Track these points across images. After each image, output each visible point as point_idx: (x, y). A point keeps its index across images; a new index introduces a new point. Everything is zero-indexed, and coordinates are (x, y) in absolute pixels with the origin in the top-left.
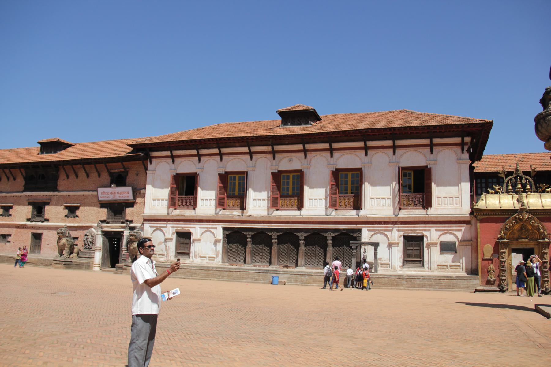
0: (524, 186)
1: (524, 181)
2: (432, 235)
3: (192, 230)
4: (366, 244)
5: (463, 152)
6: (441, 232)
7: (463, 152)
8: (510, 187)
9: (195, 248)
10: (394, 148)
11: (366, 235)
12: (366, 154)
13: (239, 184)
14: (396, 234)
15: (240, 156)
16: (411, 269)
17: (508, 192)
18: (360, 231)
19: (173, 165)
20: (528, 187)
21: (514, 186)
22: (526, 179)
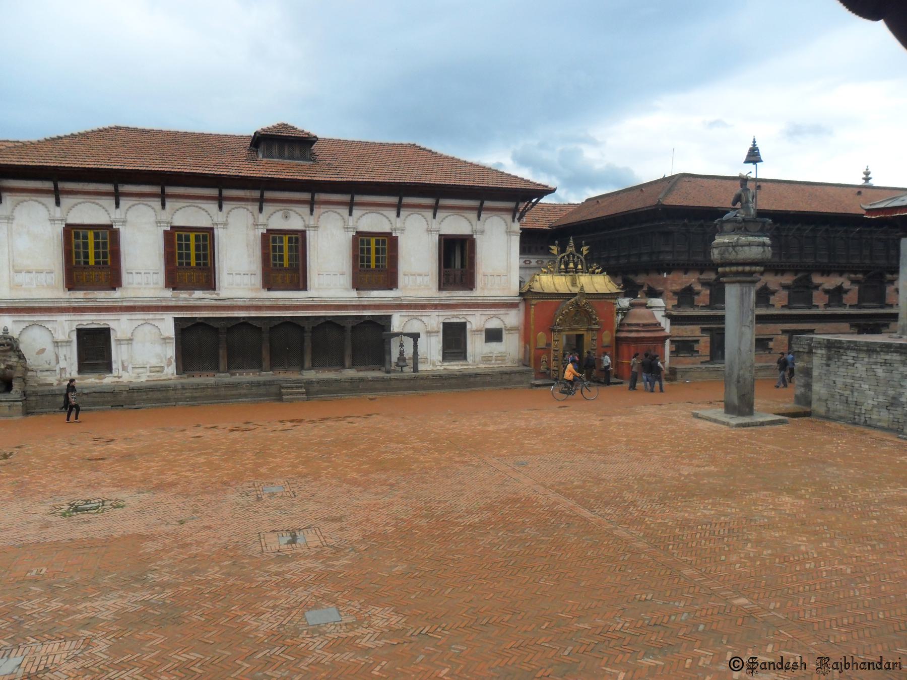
0: (576, 265)
1: (576, 259)
2: (476, 321)
3: (112, 325)
4: (397, 335)
5: (514, 221)
6: (486, 317)
7: (514, 221)
8: (563, 266)
9: (118, 354)
10: (435, 208)
11: (398, 322)
12: (398, 215)
13: (197, 248)
14: (435, 320)
15: (199, 203)
16: (452, 363)
17: (560, 272)
18: (389, 317)
19: (58, 209)
20: (580, 267)
21: (567, 264)
22: (578, 258)
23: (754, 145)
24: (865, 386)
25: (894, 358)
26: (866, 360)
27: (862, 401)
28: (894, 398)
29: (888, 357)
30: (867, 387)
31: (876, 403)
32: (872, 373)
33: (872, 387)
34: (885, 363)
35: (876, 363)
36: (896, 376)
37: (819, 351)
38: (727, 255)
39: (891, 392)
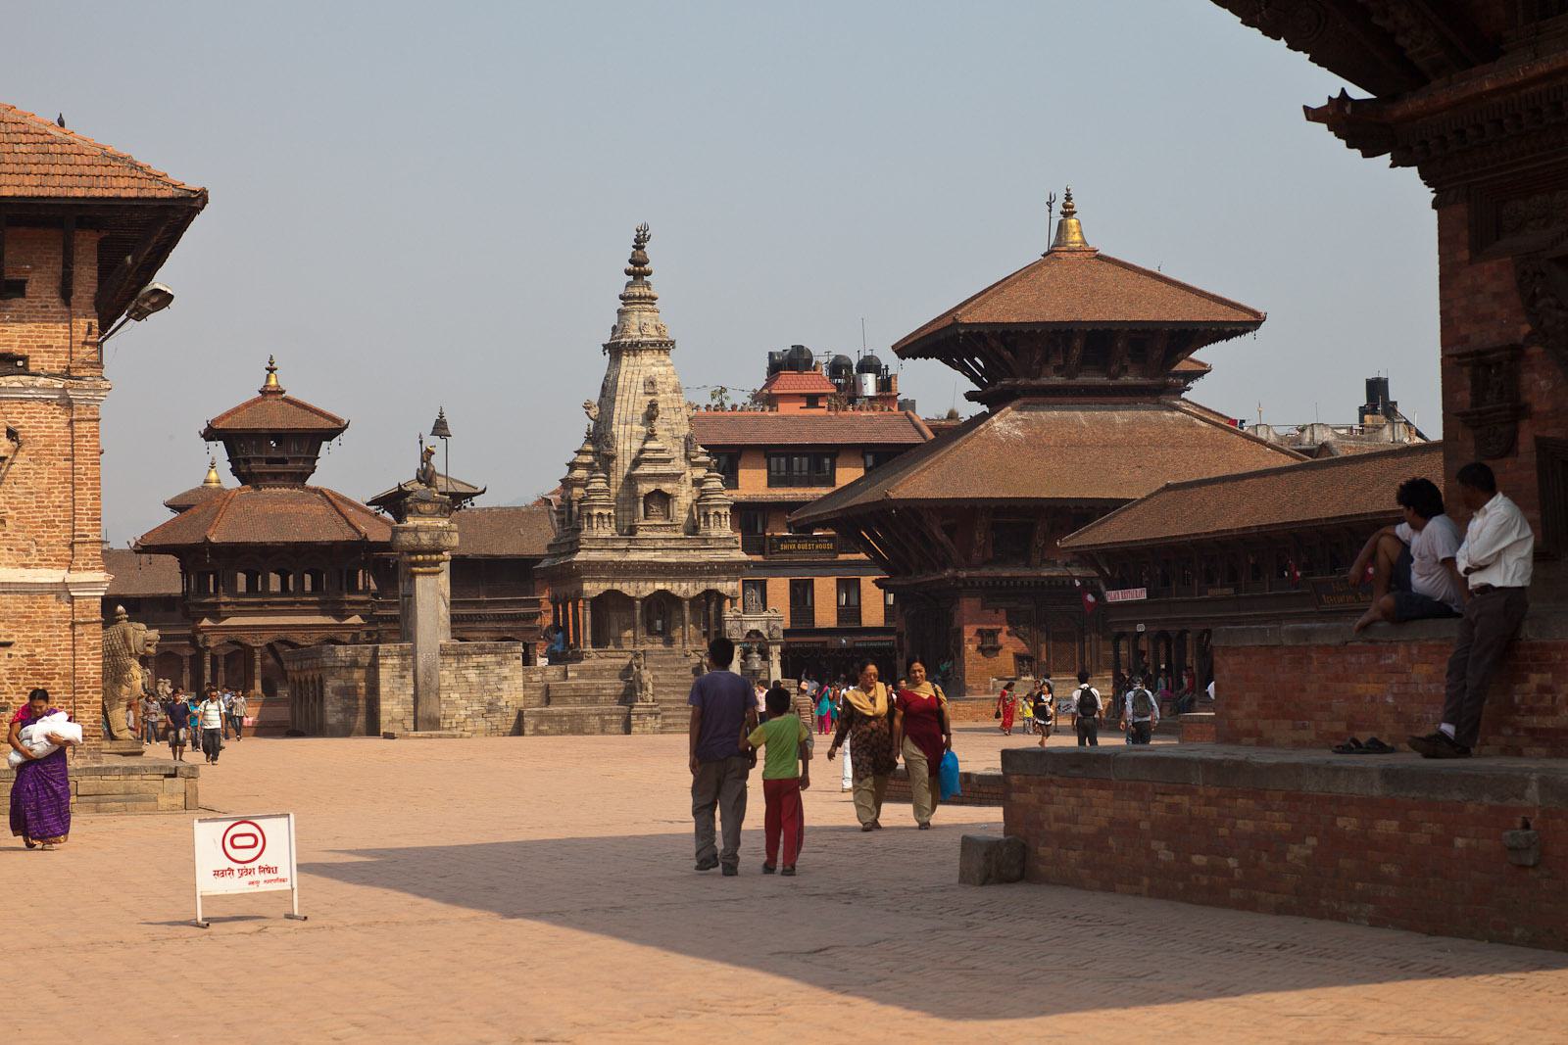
23: (441, 417)
24: (455, 696)
25: (488, 660)
26: (456, 665)
27: (453, 712)
28: (490, 704)
29: (481, 660)
30: (458, 696)
31: (470, 713)
32: (462, 679)
33: (463, 695)
34: (478, 667)
35: (467, 668)
36: (493, 679)
37: (389, 661)
38: (442, 541)
39: (487, 698)
